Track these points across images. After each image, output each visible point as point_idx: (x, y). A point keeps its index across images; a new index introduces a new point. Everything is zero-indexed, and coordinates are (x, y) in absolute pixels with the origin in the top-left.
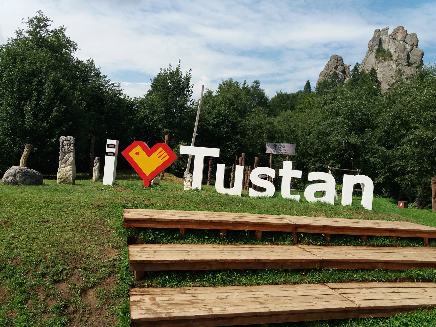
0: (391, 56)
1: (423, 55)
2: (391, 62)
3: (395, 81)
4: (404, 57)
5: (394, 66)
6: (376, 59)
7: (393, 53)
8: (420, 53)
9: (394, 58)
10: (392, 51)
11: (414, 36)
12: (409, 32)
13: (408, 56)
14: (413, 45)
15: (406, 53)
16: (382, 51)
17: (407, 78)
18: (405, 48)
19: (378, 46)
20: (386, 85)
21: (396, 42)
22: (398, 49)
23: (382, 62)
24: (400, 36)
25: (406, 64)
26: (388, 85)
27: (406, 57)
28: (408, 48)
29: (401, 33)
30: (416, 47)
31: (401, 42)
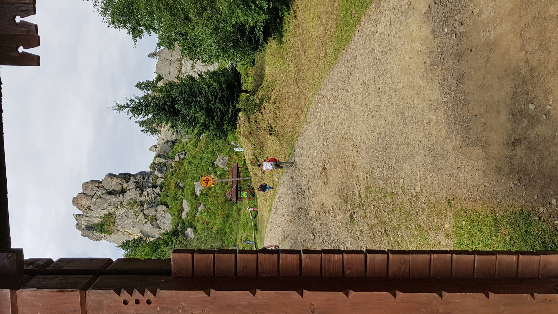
0: (110, 214)
1: (111, 175)
2: (117, 215)
3: (141, 214)
4: (112, 198)
5: (123, 210)
6: (113, 234)
7: (106, 212)
8: (109, 179)
9: (113, 210)
10: (103, 213)
11: (86, 185)
12: (81, 191)
13: (110, 193)
14: (98, 187)
15: (106, 197)
16: (101, 226)
17: (141, 196)
18: (101, 197)
19: (95, 231)
20: (146, 226)
21: (92, 208)
22: (101, 206)
23: (117, 226)
24: (86, 202)
25: (121, 196)
26: (146, 223)
27: (112, 196)
28: (101, 192)
29: (82, 200)
30: (101, 182)
31: (94, 200)
